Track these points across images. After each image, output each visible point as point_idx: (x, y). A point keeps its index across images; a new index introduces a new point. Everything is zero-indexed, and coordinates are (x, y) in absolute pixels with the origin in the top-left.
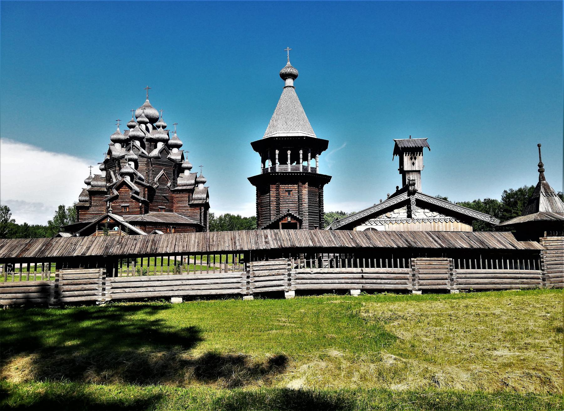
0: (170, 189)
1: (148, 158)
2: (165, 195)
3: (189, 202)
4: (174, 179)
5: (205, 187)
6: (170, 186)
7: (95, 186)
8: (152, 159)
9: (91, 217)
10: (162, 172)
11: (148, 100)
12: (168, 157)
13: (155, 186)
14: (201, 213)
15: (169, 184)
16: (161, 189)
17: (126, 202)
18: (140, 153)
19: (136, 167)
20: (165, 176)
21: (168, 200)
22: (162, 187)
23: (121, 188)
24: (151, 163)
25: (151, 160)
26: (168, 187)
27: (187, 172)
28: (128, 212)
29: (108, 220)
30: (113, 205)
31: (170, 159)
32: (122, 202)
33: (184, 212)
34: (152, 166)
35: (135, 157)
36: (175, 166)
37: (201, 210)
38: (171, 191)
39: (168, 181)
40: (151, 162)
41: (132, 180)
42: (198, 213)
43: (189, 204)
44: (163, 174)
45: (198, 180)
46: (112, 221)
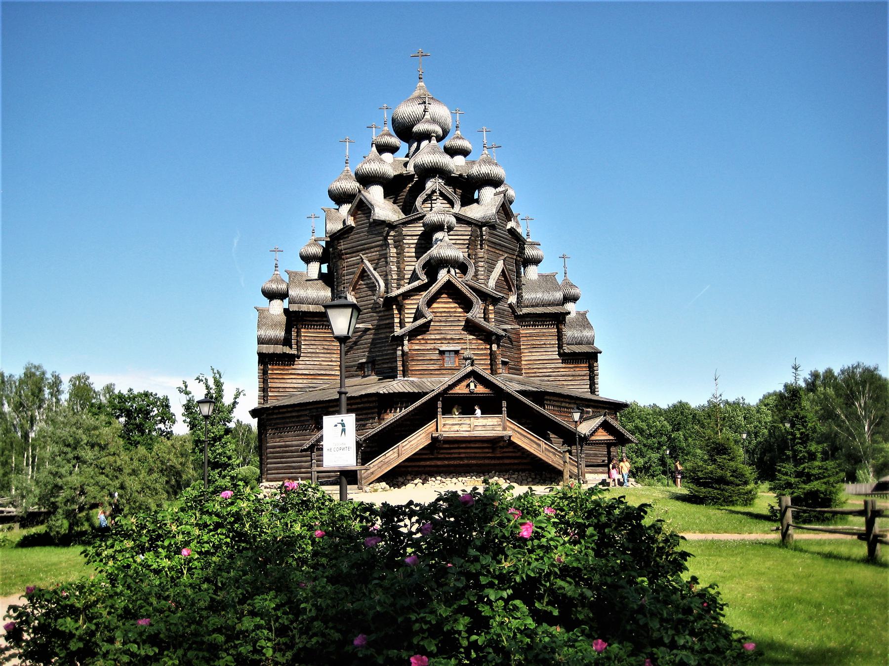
0: (514, 312)
1: (476, 225)
2: (509, 327)
3: (560, 346)
7: (301, 302)
8: (484, 229)
9: (300, 386)
11: (422, 84)
12: (508, 227)
24: (481, 241)
25: (481, 232)
26: (510, 306)
29: (472, 386)
30: (417, 347)
31: (512, 232)
33: (547, 374)
34: (481, 245)
39: (511, 290)
40: (482, 236)
42: (585, 378)
43: (559, 354)
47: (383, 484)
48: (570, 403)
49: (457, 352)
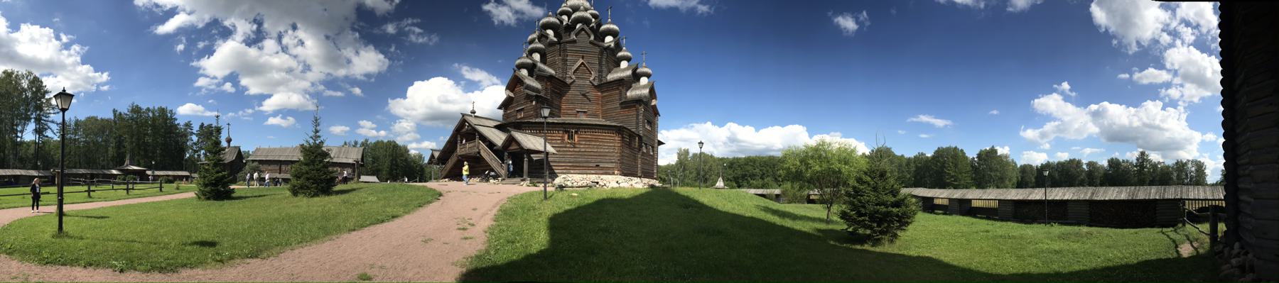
0: (593, 85)
2: (583, 93)
4: (600, 71)
5: (649, 82)
6: (594, 79)
10: (581, 61)
13: (568, 81)
14: (638, 115)
15: (591, 79)
16: (579, 86)
17: (522, 105)
18: (548, 41)
19: (543, 60)
20: (585, 66)
21: (590, 101)
22: (579, 82)
23: (515, 87)
26: (591, 82)
27: (624, 64)
28: (523, 118)
32: (517, 106)
35: (540, 45)
36: (601, 53)
37: (637, 110)
38: (595, 87)
41: (531, 74)
44: (583, 63)
45: (638, 71)
46: (470, 128)
47: (447, 180)
48: (552, 127)
49: (522, 109)
